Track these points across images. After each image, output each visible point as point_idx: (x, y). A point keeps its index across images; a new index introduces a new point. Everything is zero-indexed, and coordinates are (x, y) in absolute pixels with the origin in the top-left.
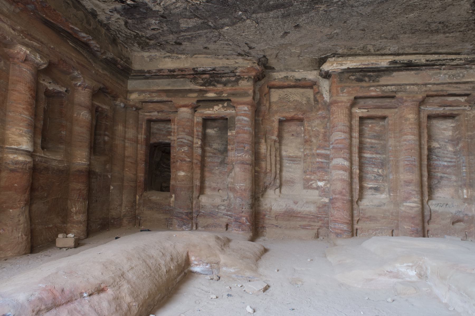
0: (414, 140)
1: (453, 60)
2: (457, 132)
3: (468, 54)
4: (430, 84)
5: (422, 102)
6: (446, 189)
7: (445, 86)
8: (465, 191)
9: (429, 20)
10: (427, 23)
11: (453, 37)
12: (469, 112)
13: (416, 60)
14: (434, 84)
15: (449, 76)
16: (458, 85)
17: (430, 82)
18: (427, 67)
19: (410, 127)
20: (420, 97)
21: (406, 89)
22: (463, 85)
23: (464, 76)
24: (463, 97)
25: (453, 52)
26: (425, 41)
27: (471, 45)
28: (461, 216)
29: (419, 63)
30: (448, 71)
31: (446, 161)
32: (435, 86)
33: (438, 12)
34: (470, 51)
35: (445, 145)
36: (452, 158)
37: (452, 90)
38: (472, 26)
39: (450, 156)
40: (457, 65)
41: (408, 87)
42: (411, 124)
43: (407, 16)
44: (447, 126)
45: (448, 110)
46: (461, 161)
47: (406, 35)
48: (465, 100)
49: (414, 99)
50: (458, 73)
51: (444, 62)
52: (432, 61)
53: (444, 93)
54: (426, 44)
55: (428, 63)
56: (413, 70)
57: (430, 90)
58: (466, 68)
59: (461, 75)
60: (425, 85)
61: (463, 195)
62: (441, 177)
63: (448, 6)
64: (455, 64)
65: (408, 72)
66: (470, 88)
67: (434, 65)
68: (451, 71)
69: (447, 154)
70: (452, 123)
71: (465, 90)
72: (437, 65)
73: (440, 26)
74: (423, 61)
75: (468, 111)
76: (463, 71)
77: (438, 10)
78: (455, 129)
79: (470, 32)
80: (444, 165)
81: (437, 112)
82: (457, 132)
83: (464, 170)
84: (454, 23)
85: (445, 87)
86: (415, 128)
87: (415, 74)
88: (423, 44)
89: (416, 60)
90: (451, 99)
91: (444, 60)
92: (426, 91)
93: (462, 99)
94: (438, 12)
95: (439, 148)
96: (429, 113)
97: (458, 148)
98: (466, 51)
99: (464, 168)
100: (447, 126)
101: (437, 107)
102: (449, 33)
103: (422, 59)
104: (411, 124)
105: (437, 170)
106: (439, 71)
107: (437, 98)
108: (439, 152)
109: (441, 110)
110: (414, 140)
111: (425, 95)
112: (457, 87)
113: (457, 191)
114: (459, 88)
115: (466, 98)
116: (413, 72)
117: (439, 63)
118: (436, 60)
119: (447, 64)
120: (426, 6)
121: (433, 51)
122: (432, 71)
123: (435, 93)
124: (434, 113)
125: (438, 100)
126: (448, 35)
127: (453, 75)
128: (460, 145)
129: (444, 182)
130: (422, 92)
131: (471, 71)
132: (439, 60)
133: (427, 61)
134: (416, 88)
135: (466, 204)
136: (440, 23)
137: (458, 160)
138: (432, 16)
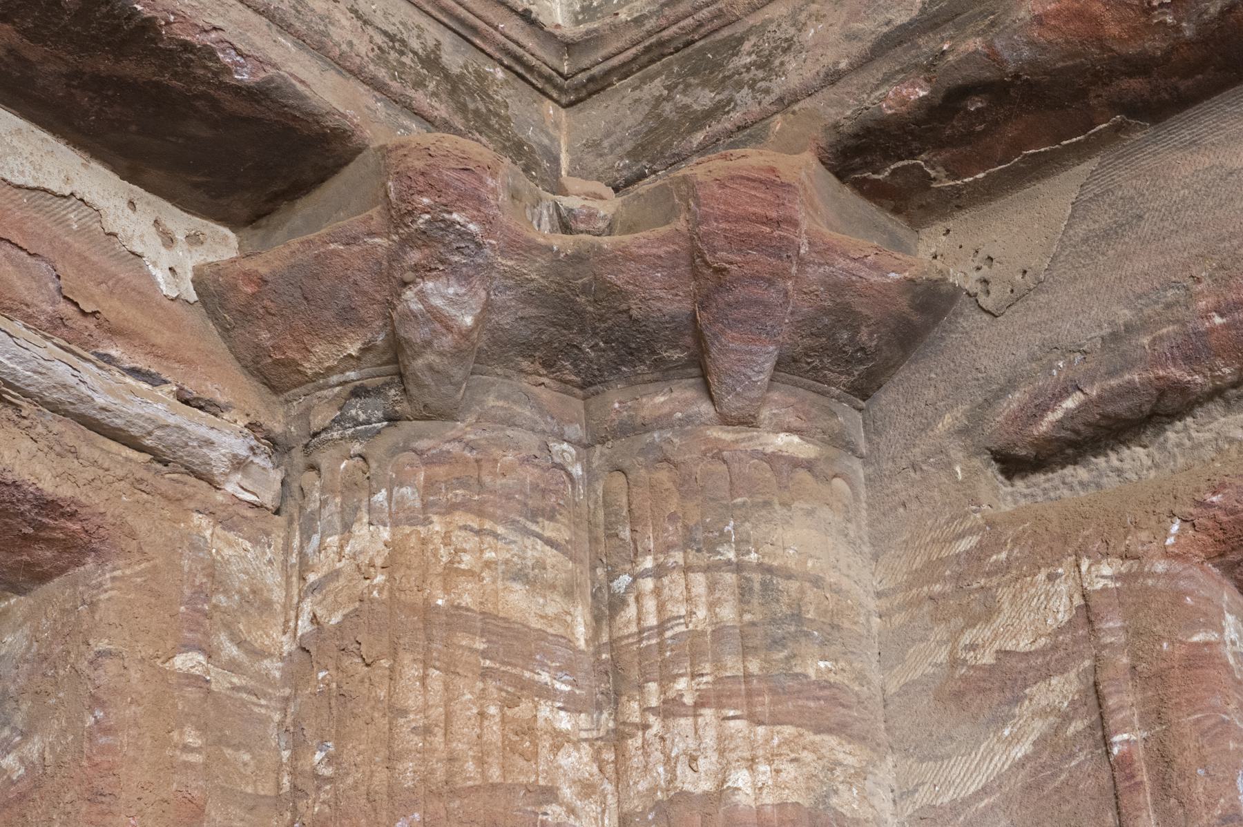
12: (237, 553)
48: (212, 292)
75: (227, 520)
115: (222, 245)
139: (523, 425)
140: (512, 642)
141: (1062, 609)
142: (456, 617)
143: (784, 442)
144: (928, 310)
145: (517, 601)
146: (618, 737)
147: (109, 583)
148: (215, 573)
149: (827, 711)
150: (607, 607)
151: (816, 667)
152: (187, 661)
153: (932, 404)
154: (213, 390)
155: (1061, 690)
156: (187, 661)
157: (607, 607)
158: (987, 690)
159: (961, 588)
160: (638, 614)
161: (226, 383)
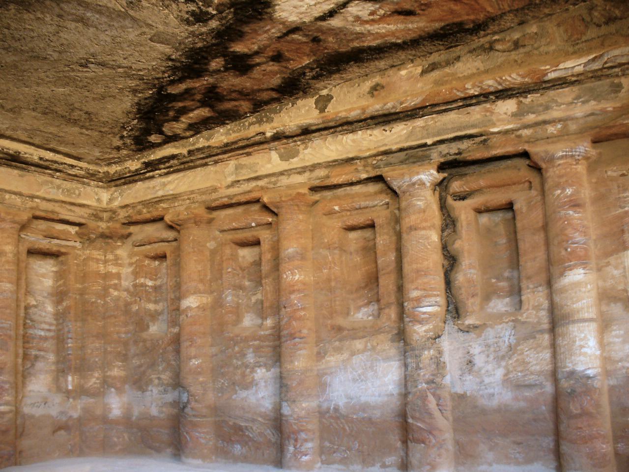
0: (11, 292)
1: (73, 166)
2: (61, 282)
3: (89, 163)
4: (38, 197)
5: (24, 227)
6: (42, 377)
7: (57, 204)
8: (70, 378)
9: (76, 105)
10: (71, 107)
11: (87, 135)
12: (79, 252)
13: (25, 153)
14: (44, 199)
15: (63, 190)
16: (73, 208)
17: (38, 194)
18: (37, 169)
19: (7, 267)
20: (25, 216)
21: (4, 199)
22: (79, 208)
23: (79, 194)
24: (74, 227)
25: (75, 155)
26: (52, 129)
27: (100, 152)
28: (64, 419)
29: (28, 160)
30: (62, 181)
31: (43, 330)
32: (44, 203)
33: (94, 99)
34: (94, 158)
35: (44, 303)
36: (51, 324)
37: (66, 215)
38: (116, 129)
39: (49, 321)
40: (76, 176)
41: (7, 196)
42: (8, 262)
43: (54, 89)
44: (47, 269)
45: (53, 245)
46: (66, 330)
47: (34, 114)
48: (76, 233)
49: (17, 218)
50: (73, 188)
51: (61, 167)
52: (47, 160)
53: (55, 217)
54: (50, 133)
55: (42, 162)
56: (16, 168)
57: (37, 208)
58: (84, 183)
59: (77, 192)
60: (32, 197)
61: (67, 386)
62: (36, 357)
63: (110, 97)
64: (74, 173)
65: (10, 170)
66: (86, 216)
67: (47, 168)
68: (65, 182)
69: (45, 317)
70: (54, 266)
71: (80, 217)
72: (51, 169)
73: (84, 116)
74: (36, 159)
75: (78, 250)
76: (80, 186)
77: (95, 96)
78: (60, 275)
79: (110, 135)
80: (41, 335)
81: (41, 246)
82: (61, 282)
83: (69, 345)
84: (102, 119)
85: (57, 208)
86: (13, 270)
87: (20, 176)
88: (46, 133)
89: (25, 153)
90: (60, 227)
91: (62, 164)
92: (32, 208)
93: (73, 230)
94: (94, 99)
95: (35, 306)
96: (30, 245)
97: (60, 307)
98: (90, 157)
99: (70, 341)
100: (47, 269)
101: (41, 237)
102: (87, 129)
103: (33, 154)
104: (8, 262)
105: (31, 345)
106: (50, 179)
107: (42, 222)
108: (35, 314)
109: (44, 244)
110: (11, 292)
111: (31, 215)
112: (71, 210)
113: (56, 380)
114: (74, 212)
115: (77, 228)
116: (16, 172)
117: (55, 166)
118: (52, 161)
119: (65, 171)
120: (86, 86)
121: (51, 146)
122: (42, 177)
123: (43, 214)
124: (36, 247)
125: (42, 225)
126: (84, 131)
127: (68, 191)
128: (64, 304)
129: (40, 365)
130: (26, 209)
131: (88, 189)
132: (56, 162)
133: (41, 159)
134: (18, 200)
135: (71, 400)
136: (86, 113)
137: (60, 327)
138: (83, 102)
139: (100, 243)
140: (98, 260)
141: (135, 260)
142: (94, 258)
143: (119, 244)
144: (129, 235)
145: (99, 257)
146: (105, 266)
147: (70, 257)
148: (77, 254)
149: (121, 265)
150: (105, 256)
151: (120, 262)
152: (76, 261)
153: (130, 241)
154: (77, 240)
155: (135, 265)
156: (76, 261)
157: (105, 256)
158: (131, 264)
159: (130, 256)
160: (107, 257)
161: (78, 240)
